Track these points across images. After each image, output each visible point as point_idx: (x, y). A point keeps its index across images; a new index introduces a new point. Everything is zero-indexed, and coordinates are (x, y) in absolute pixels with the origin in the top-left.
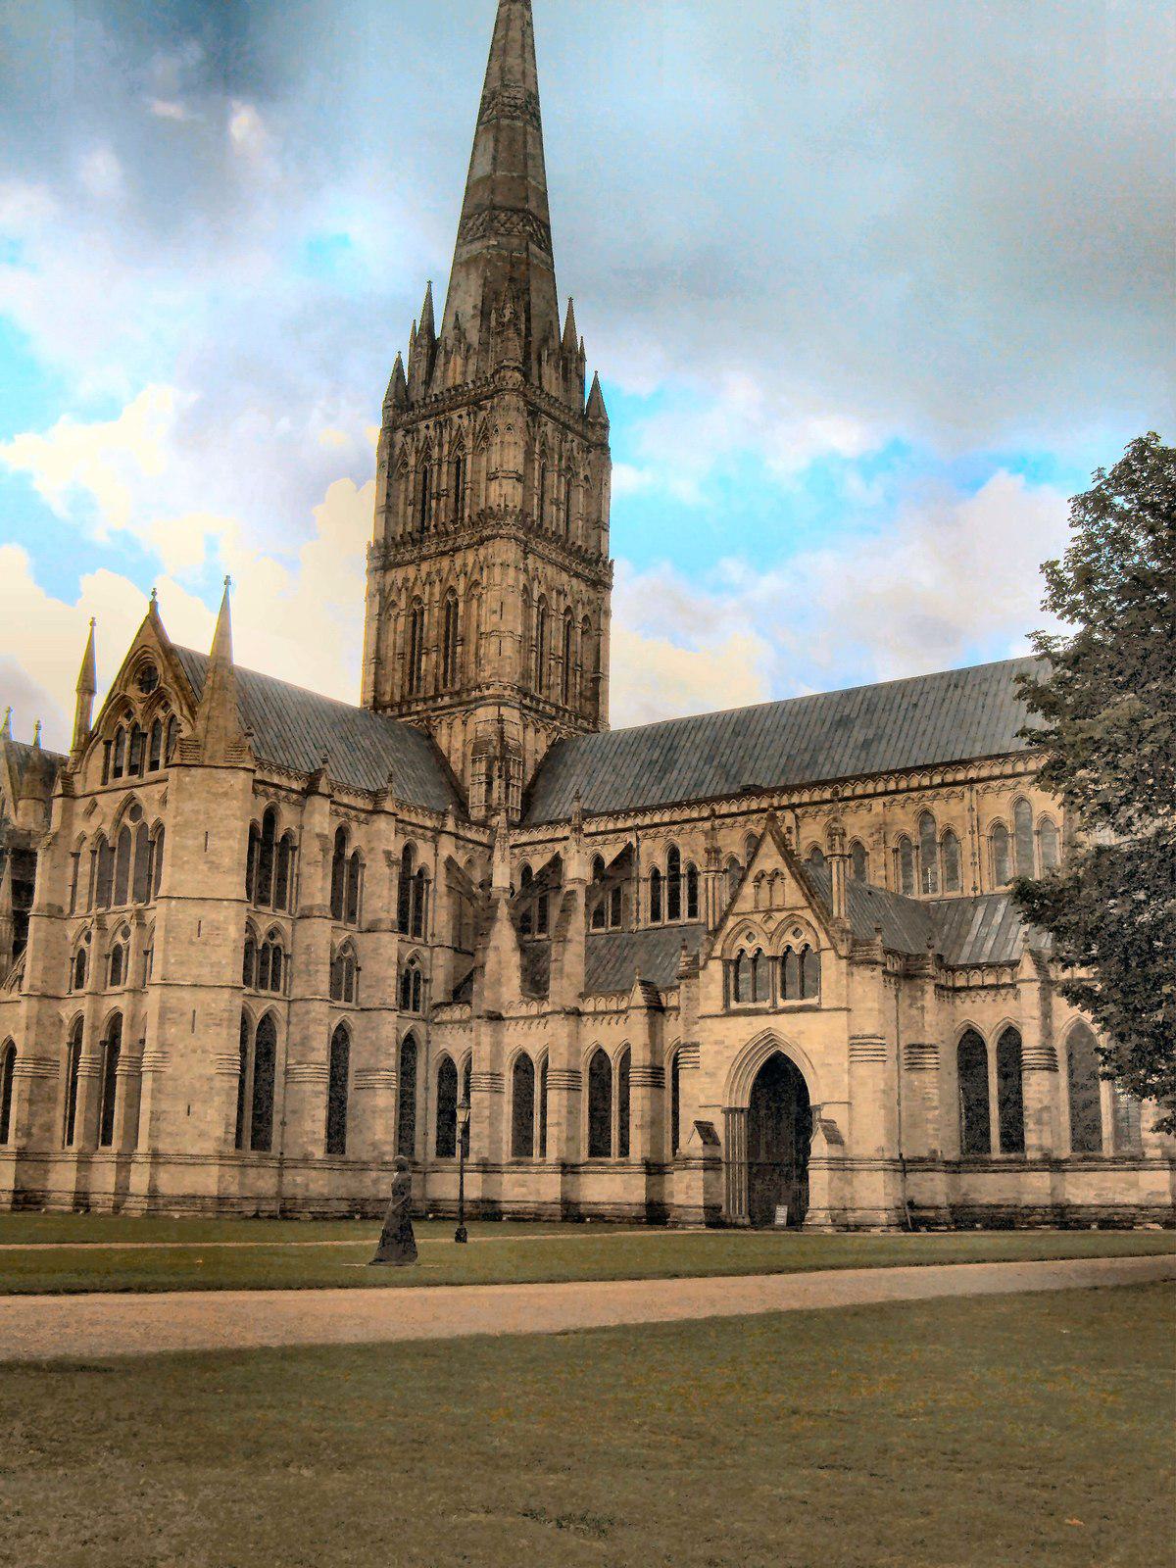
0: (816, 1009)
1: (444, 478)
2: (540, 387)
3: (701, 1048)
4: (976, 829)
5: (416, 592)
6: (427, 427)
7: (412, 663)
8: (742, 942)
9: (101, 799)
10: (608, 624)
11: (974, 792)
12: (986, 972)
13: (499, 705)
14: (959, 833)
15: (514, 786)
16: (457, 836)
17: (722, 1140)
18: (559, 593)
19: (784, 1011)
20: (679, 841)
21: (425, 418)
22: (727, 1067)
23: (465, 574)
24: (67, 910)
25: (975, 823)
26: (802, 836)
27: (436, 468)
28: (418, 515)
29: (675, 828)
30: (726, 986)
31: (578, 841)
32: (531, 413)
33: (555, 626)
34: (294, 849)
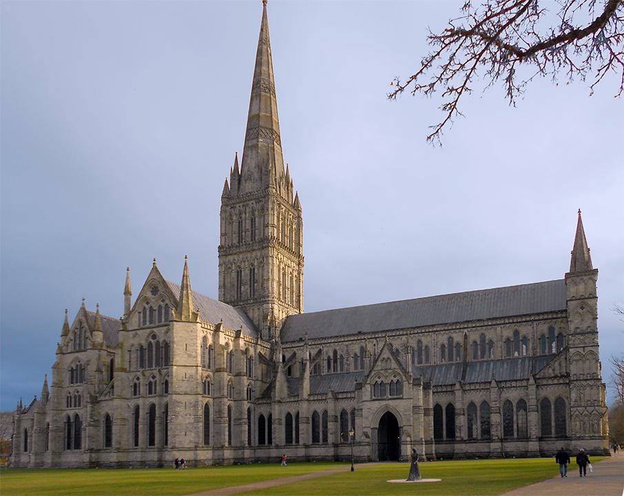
19: (391, 399)
21: (239, 203)
22: (372, 416)
28: (237, 238)
31: (307, 347)
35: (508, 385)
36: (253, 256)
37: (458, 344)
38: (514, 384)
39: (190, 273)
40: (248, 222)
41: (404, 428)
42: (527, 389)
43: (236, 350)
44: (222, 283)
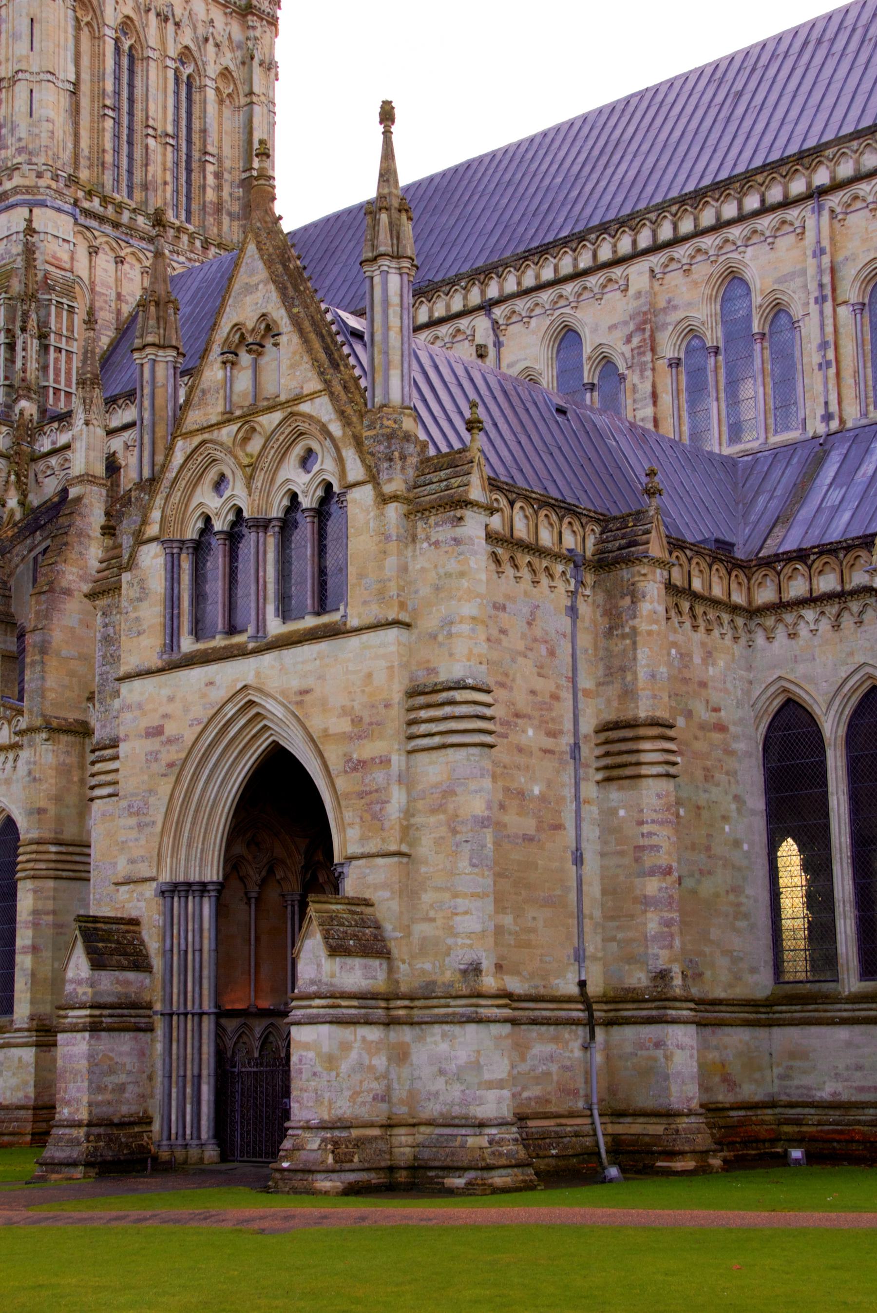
3: (123, 749)
4: (828, 291)
10: (270, 87)
11: (826, 214)
12: (818, 565)
13: (31, 206)
14: (796, 311)
15: (59, 350)
17: (157, 963)
18: (163, 18)
22: (165, 788)
25: (827, 279)
26: (508, 356)
30: (172, 601)
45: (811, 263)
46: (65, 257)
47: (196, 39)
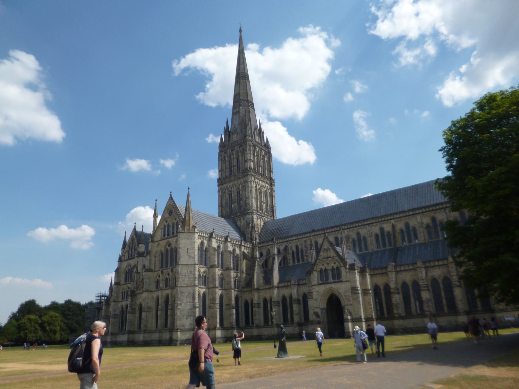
0: (341, 282)
1: (234, 162)
2: (255, 140)
3: (313, 293)
5: (230, 189)
6: (229, 151)
7: (230, 206)
8: (321, 266)
9: (161, 242)
16: (244, 246)
20: (298, 244)
21: (229, 149)
23: (241, 184)
24: (154, 270)
25: (370, 234)
27: (232, 160)
28: (229, 171)
29: (297, 240)
32: (253, 146)
33: (263, 195)
34: (208, 251)
35: (432, 264)
36: (239, 182)
37: (388, 233)
38: (436, 263)
39: (191, 199)
40: (235, 160)
41: (346, 308)
42: (448, 267)
43: (225, 251)
44: (220, 203)
45: (368, 232)
46: (256, 220)
47: (266, 189)
